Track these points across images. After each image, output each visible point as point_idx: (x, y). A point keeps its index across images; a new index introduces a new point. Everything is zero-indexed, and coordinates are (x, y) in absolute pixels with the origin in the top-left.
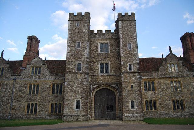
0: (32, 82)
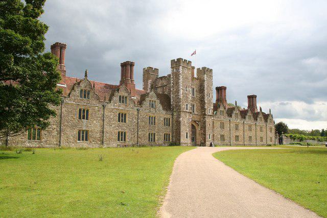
0: (151, 115)
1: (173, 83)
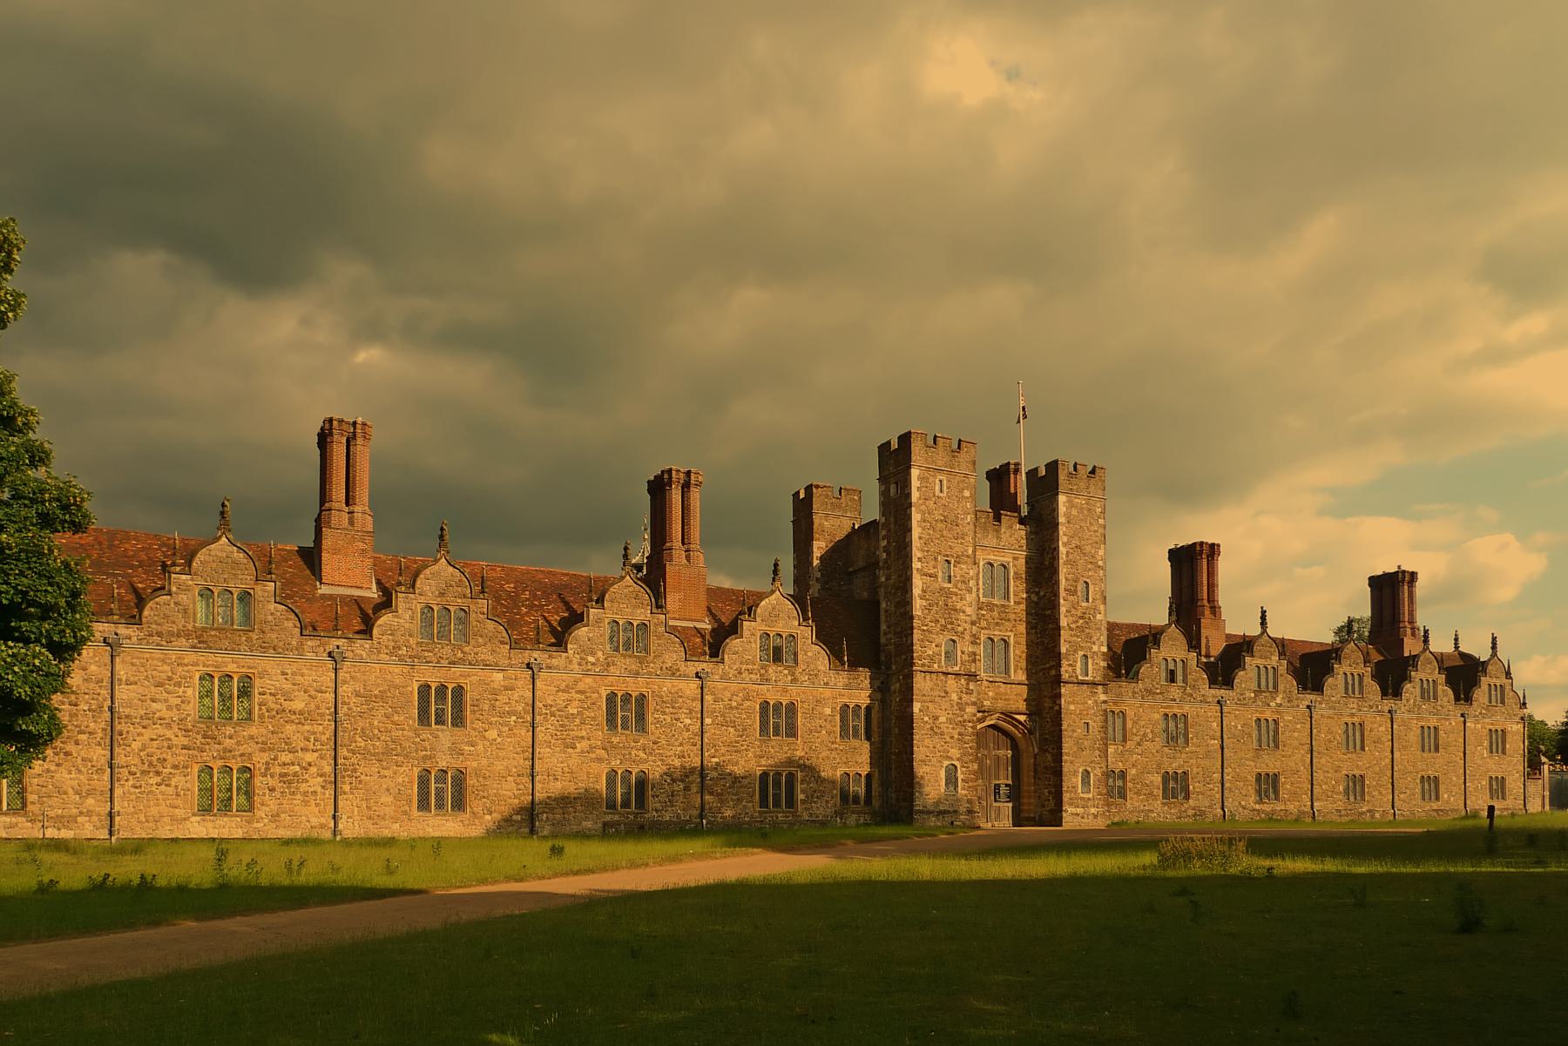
1: (886, 549)
